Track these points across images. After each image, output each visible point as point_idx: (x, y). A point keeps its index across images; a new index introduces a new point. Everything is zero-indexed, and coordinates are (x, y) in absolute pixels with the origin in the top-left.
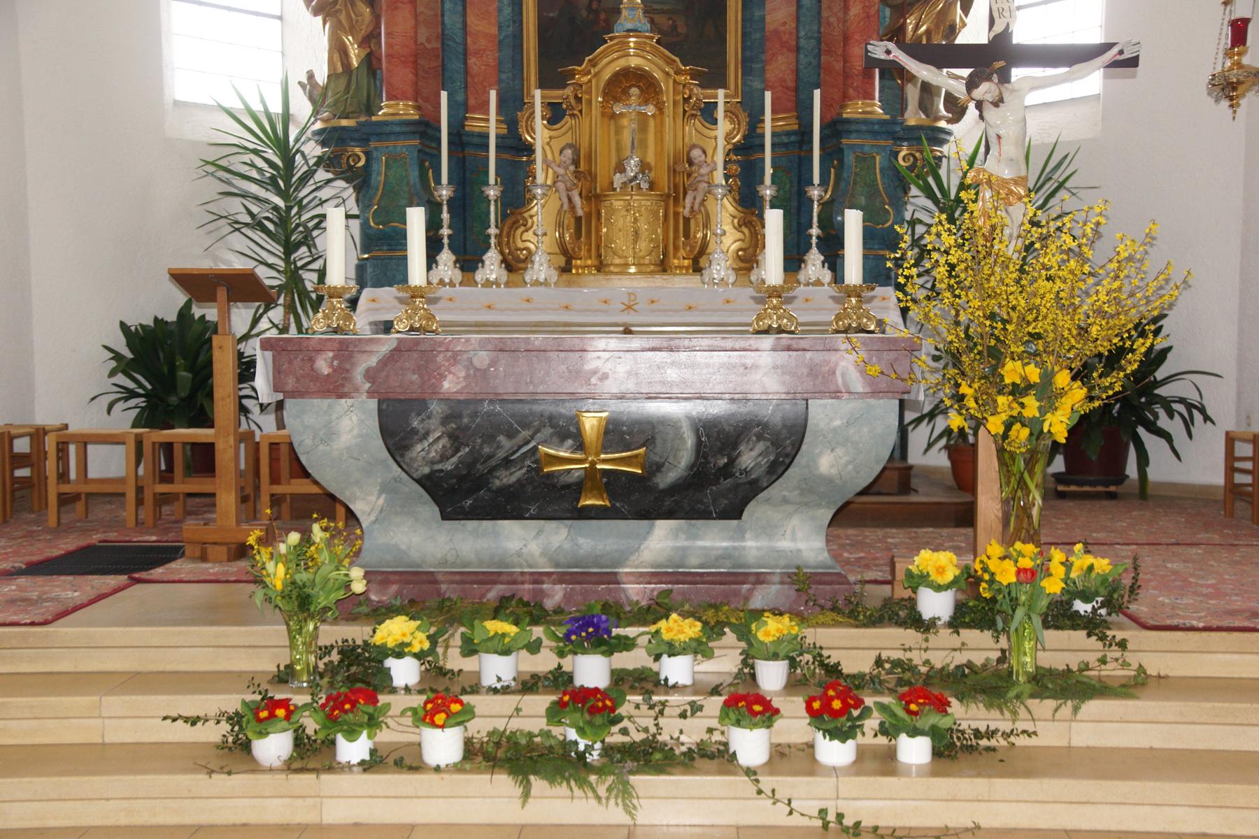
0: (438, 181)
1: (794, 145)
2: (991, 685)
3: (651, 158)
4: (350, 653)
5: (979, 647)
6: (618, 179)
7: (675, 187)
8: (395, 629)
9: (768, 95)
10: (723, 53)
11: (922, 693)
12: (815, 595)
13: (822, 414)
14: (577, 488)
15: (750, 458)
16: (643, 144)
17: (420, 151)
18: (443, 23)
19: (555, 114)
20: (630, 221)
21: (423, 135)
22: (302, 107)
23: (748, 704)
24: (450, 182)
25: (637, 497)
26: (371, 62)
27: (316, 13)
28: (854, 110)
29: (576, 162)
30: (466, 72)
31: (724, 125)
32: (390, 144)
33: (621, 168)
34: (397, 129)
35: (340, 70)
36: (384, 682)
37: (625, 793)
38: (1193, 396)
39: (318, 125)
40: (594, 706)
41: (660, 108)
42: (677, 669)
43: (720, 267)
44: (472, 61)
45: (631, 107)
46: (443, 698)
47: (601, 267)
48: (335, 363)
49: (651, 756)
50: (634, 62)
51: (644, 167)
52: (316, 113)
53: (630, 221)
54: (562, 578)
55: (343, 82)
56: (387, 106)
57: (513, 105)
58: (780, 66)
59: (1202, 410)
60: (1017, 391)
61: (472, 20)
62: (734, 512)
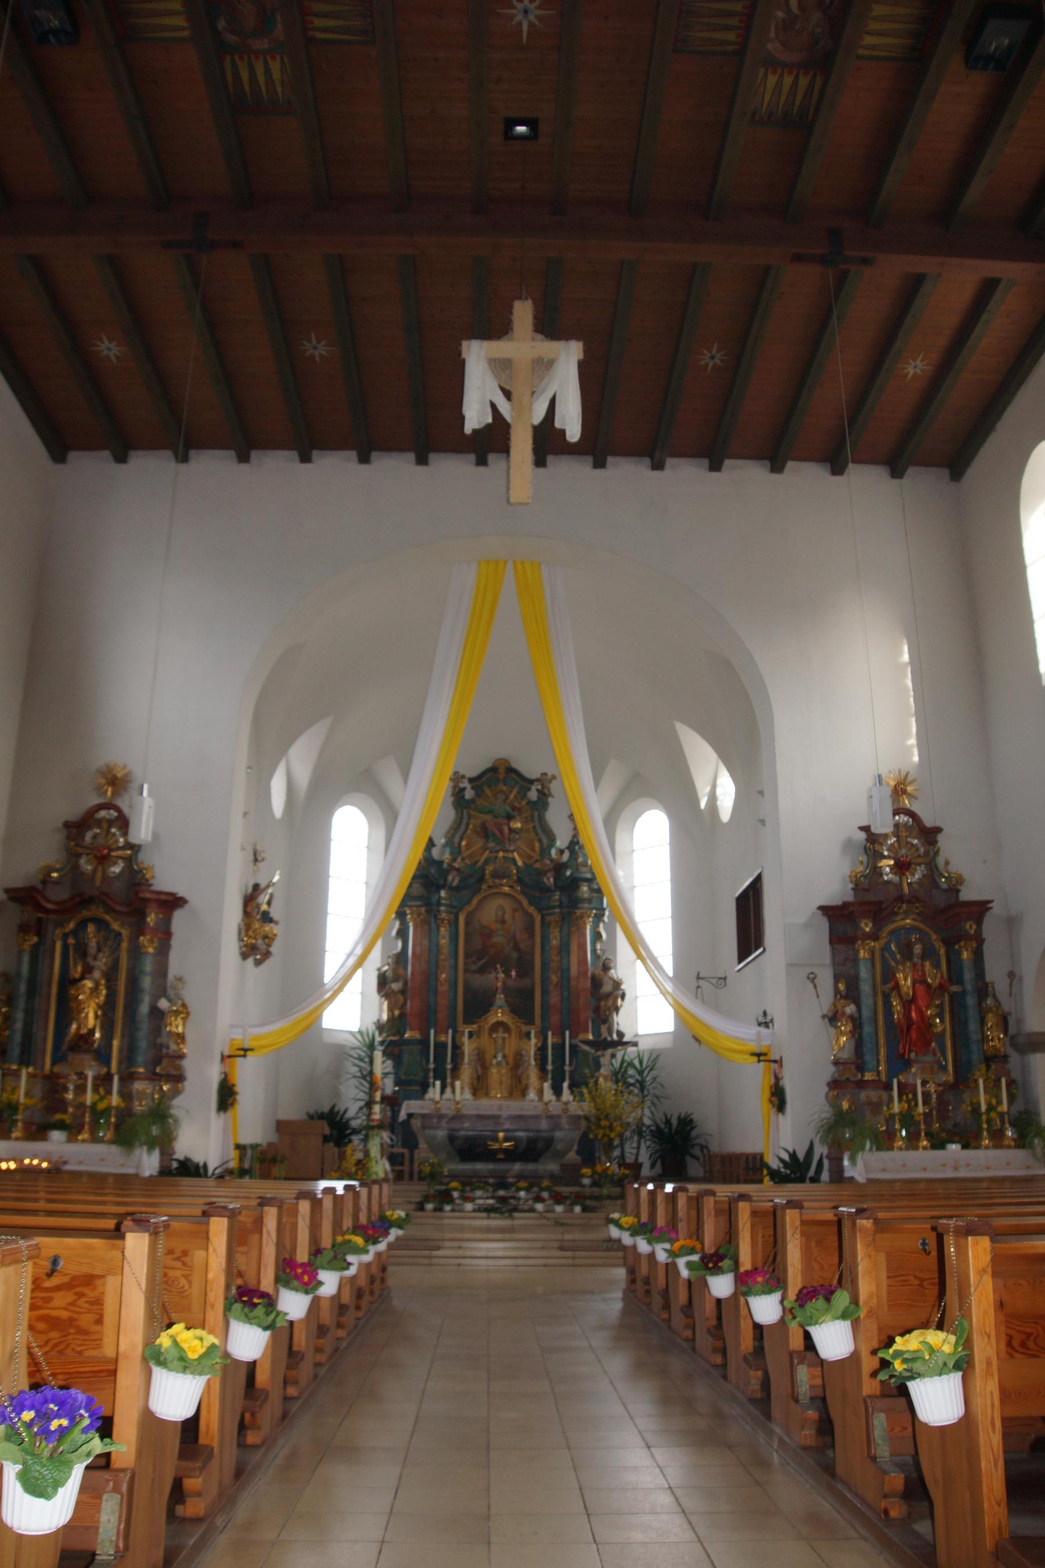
0: (428, 1061)
2: (598, 1198)
3: (507, 1052)
4: (440, 1192)
5: (596, 1191)
6: (494, 1062)
7: (517, 1064)
8: (454, 1184)
9: (550, 1033)
10: (533, 1013)
11: (579, 1199)
12: (554, 1178)
13: (558, 1134)
14: (495, 1152)
15: (540, 1145)
16: (504, 1047)
19: (471, 1034)
20: (497, 1074)
23: (538, 1199)
25: (511, 1156)
26: (402, 1015)
29: (478, 1054)
31: (533, 1041)
33: (495, 1057)
36: (451, 1196)
37: (512, 1218)
38: (704, 1143)
40: (503, 1200)
41: (510, 1034)
42: (522, 1194)
43: (532, 1095)
44: (440, 1016)
45: (500, 1034)
46: (466, 1199)
47: (487, 1094)
49: (516, 1209)
50: (500, 1019)
51: (504, 1057)
53: (497, 1074)
54: (492, 1177)
58: (555, 1019)
59: (707, 1148)
60: (603, 1128)
62: (535, 1160)
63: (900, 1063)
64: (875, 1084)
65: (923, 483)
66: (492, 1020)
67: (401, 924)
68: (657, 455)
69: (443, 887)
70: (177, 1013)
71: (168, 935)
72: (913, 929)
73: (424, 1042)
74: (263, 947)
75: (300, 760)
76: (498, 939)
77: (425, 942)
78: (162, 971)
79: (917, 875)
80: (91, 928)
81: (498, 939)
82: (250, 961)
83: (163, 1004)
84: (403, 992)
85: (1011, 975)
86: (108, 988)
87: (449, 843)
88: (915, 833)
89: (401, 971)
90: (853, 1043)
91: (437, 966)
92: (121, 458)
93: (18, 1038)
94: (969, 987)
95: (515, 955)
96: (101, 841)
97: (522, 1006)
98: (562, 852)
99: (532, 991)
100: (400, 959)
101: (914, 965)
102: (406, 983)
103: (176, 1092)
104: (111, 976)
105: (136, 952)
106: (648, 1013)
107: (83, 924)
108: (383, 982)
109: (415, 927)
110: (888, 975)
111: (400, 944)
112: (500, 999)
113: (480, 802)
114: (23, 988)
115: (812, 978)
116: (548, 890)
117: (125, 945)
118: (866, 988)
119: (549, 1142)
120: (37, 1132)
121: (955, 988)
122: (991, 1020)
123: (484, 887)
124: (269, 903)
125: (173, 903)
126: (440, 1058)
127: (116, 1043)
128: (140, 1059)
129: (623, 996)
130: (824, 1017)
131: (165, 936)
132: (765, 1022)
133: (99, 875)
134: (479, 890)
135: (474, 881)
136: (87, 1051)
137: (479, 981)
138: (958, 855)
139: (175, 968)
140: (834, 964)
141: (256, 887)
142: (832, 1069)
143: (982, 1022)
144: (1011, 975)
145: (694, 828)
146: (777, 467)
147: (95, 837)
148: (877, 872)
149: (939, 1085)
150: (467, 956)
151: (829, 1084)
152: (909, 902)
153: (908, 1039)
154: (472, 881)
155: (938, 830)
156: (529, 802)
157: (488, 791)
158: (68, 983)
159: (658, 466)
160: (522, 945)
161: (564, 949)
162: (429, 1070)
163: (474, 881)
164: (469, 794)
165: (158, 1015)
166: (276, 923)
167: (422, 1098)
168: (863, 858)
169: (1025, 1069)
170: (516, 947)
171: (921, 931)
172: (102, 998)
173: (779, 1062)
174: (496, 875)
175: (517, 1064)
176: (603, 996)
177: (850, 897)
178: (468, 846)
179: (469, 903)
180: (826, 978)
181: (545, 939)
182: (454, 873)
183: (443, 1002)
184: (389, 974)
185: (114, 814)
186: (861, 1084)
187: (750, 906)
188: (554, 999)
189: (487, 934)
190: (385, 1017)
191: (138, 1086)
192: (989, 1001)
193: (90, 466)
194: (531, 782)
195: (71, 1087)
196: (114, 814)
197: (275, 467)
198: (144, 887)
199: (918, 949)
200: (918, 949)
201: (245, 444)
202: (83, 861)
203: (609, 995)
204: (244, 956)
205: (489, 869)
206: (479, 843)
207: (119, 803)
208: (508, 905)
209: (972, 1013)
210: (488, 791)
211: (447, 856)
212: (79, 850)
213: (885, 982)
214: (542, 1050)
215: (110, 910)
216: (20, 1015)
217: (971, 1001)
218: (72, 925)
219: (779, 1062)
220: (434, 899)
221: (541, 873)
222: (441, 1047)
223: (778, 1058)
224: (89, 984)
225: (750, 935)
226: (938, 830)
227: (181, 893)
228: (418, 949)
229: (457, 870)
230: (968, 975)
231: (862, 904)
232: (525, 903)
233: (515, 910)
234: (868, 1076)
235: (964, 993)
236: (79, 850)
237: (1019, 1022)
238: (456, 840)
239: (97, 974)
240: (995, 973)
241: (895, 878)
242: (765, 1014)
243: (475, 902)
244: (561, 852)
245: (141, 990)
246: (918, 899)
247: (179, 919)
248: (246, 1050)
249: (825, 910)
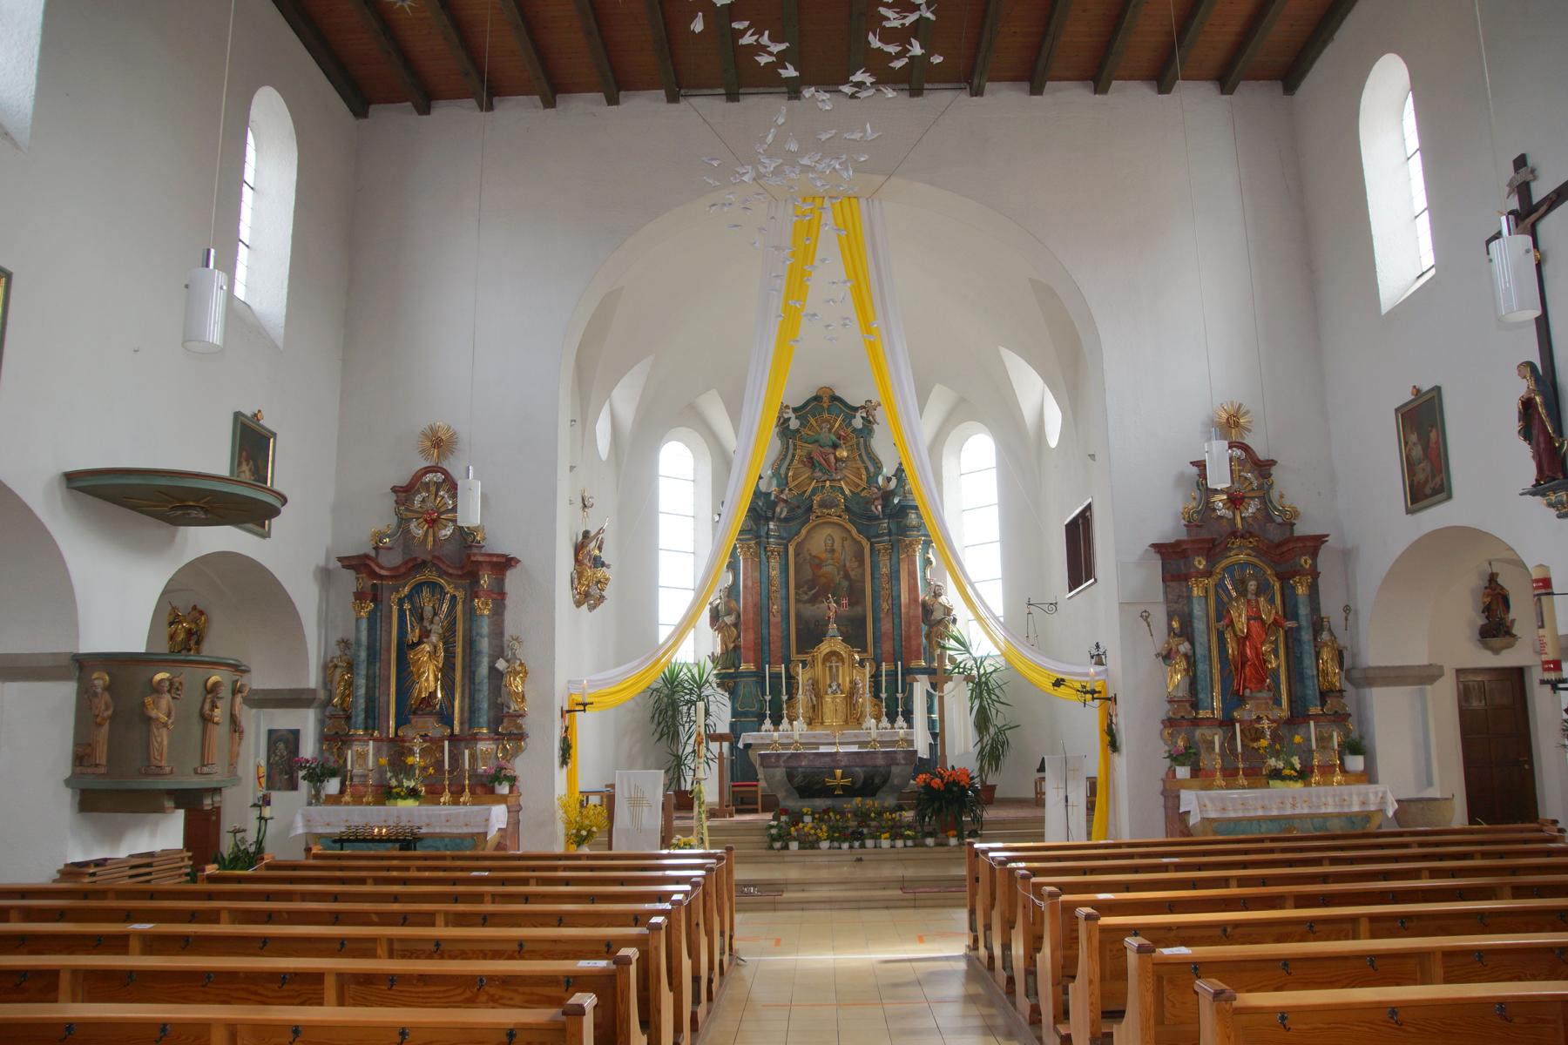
0: (764, 694)
1: (892, 675)
13: (895, 769)
15: (877, 780)
22: (709, 665)
25: (850, 792)
26: (737, 648)
28: (913, 664)
53: (832, 703)
57: (788, 661)
58: (887, 646)
63: (1235, 699)
64: (1210, 722)
65: (1255, 96)
66: (825, 648)
68: (976, 81)
69: (772, 519)
70: (517, 673)
71: (502, 595)
72: (1247, 564)
73: (759, 674)
74: (594, 591)
75: (624, 399)
76: (827, 569)
78: (498, 632)
79: (1251, 509)
80: (426, 592)
81: (827, 569)
82: (585, 607)
83: (501, 665)
84: (736, 625)
85: (1347, 609)
86: (446, 651)
87: (776, 474)
88: (1248, 466)
89: (733, 604)
90: (1187, 681)
91: (769, 598)
92: (424, 110)
93: (362, 703)
94: (1304, 622)
95: (845, 583)
96: (429, 504)
97: (854, 634)
98: (889, 480)
99: (863, 620)
100: (732, 592)
101: (1249, 601)
103: (518, 751)
104: (448, 639)
105: (471, 615)
106: (978, 639)
107: (418, 588)
109: (745, 560)
110: (1222, 612)
112: (833, 627)
113: (804, 431)
114: (363, 654)
115: (1145, 616)
116: (877, 518)
117: (459, 607)
118: (1199, 626)
119: (886, 779)
120: (385, 794)
121: (1289, 624)
122: (1326, 654)
123: (812, 517)
124: (600, 548)
125: (505, 564)
126: (775, 690)
127: (457, 703)
128: (484, 719)
129: (954, 621)
130: (1158, 655)
131: (499, 596)
132: (1099, 659)
133: (430, 539)
134: (808, 520)
135: (801, 512)
136: (430, 714)
137: (810, 611)
138: (1291, 488)
139: (510, 629)
140: (1167, 601)
141: (586, 534)
142: (1167, 706)
143: (1318, 655)
144: (1347, 609)
145: (1021, 456)
146: (1100, 87)
147: (423, 501)
148: (1209, 507)
149: (1273, 721)
150: (797, 587)
151: (1163, 722)
152: (1242, 537)
153: (1243, 674)
154: (800, 511)
155: (1272, 463)
156: (855, 430)
157: (812, 421)
158: (405, 647)
159: (977, 92)
160: (852, 574)
161: (894, 576)
163: (801, 512)
164: (794, 424)
165: (496, 676)
166: (608, 567)
168: (1196, 493)
169: (1361, 704)
170: (847, 576)
171: (1255, 566)
172: (441, 660)
173: (1114, 699)
174: (823, 504)
175: (852, 693)
176: (934, 620)
177: (1182, 534)
178: (795, 477)
179: (798, 533)
180: (1159, 614)
181: (875, 566)
182: (782, 505)
183: (775, 633)
185: (440, 477)
186: (1196, 722)
187: (1079, 533)
188: (886, 626)
189: (817, 564)
190: (718, 651)
191: (483, 746)
192: (1325, 636)
193: (394, 119)
194: (856, 409)
195: (417, 750)
196: (440, 477)
197: (583, 112)
198: (475, 550)
199: (1252, 586)
200: (1252, 586)
201: (553, 86)
202: (413, 526)
203: (940, 621)
204: (578, 604)
205: (816, 499)
206: (807, 473)
207: (445, 465)
208: (837, 534)
209: (1308, 648)
210: (812, 421)
211: (774, 488)
212: (410, 515)
213: (1219, 618)
214: (876, 677)
215: (442, 573)
216: (362, 682)
217: (1306, 636)
218: (407, 590)
219: (1114, 699)
220: (763, 533)
221: (869, 502)
222: (776, 677)
223: (1111, 695)
224: (427, 648)
225: (1080, 567)
226: (1272, 463)
227: (512, 552)
228: (750, 583)
229: (786, 501)
230: (1303, 611)
231: (1194, 542)
232: (854, 531)
233: (844, 539)
234: (1202, 714)
235: (1299, 628)
236: (410, 515)
237: (1354, 656)
238: (783, 471)
239: (434, 638)
240: (1330, 607)
241: (1228, 514)
242: (1098, 646)
243: (804, 532)
244: (889, 480)
245: (479, 653)
246: (1252, 535)
247: (511, 577)
248: (585, 705)
249: (1158, 547)
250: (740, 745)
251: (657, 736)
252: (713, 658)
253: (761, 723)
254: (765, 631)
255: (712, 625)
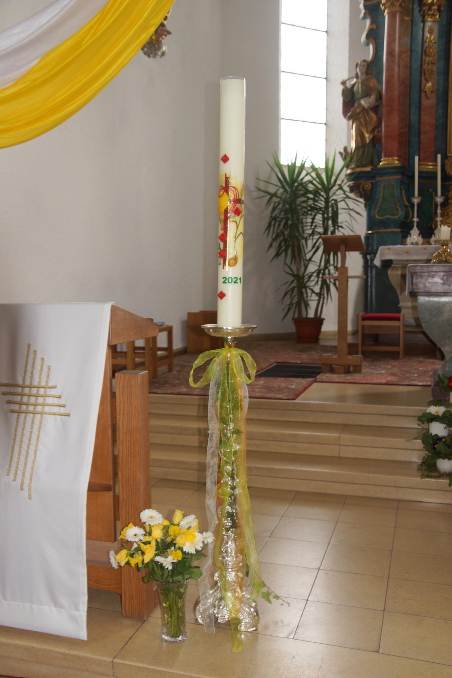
17: (401, 182)
18: (410, 119)
21: (403, 174)
22: (340, 163)
24: (419, 195)
26: (376, 140)
27: (349, 119)
30: (420, 142)
32: (386, 178)
34: (391, 171)
35: (360, 145)
39: (349, 171)
44: (422, 137)
48: (445, 278)
52: (347, 166)
55: (361, 151)
56: (384, 160)
61: (423, 117)
67: (372, 23)
73: (405, 172)
77: (407, 40)
84: (376, 109)
89: (373, 83)
91: (422, 72)
102: (380, 97)
108: (350, 100)
109: (392, 16)
111: (371, 47)
162: (412, 205)
167: (403, 242)
183: (428, 119)
184: (358, 89)
190: (353, 145)
250: (377, 262)
251: (273, 252)
252: (345, 154)
253: (406, 234)
254: (414, 118)
255: (345, 113)
